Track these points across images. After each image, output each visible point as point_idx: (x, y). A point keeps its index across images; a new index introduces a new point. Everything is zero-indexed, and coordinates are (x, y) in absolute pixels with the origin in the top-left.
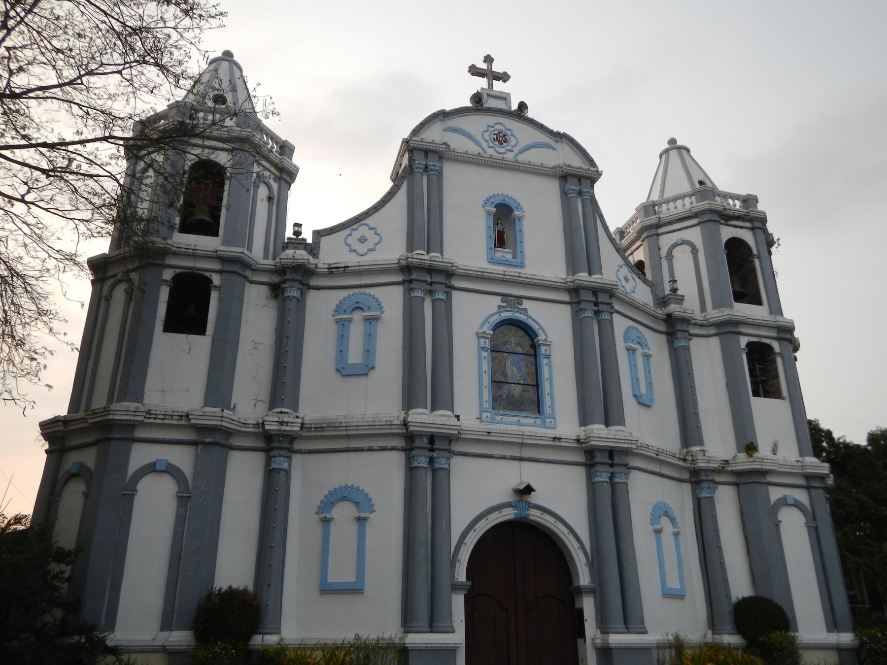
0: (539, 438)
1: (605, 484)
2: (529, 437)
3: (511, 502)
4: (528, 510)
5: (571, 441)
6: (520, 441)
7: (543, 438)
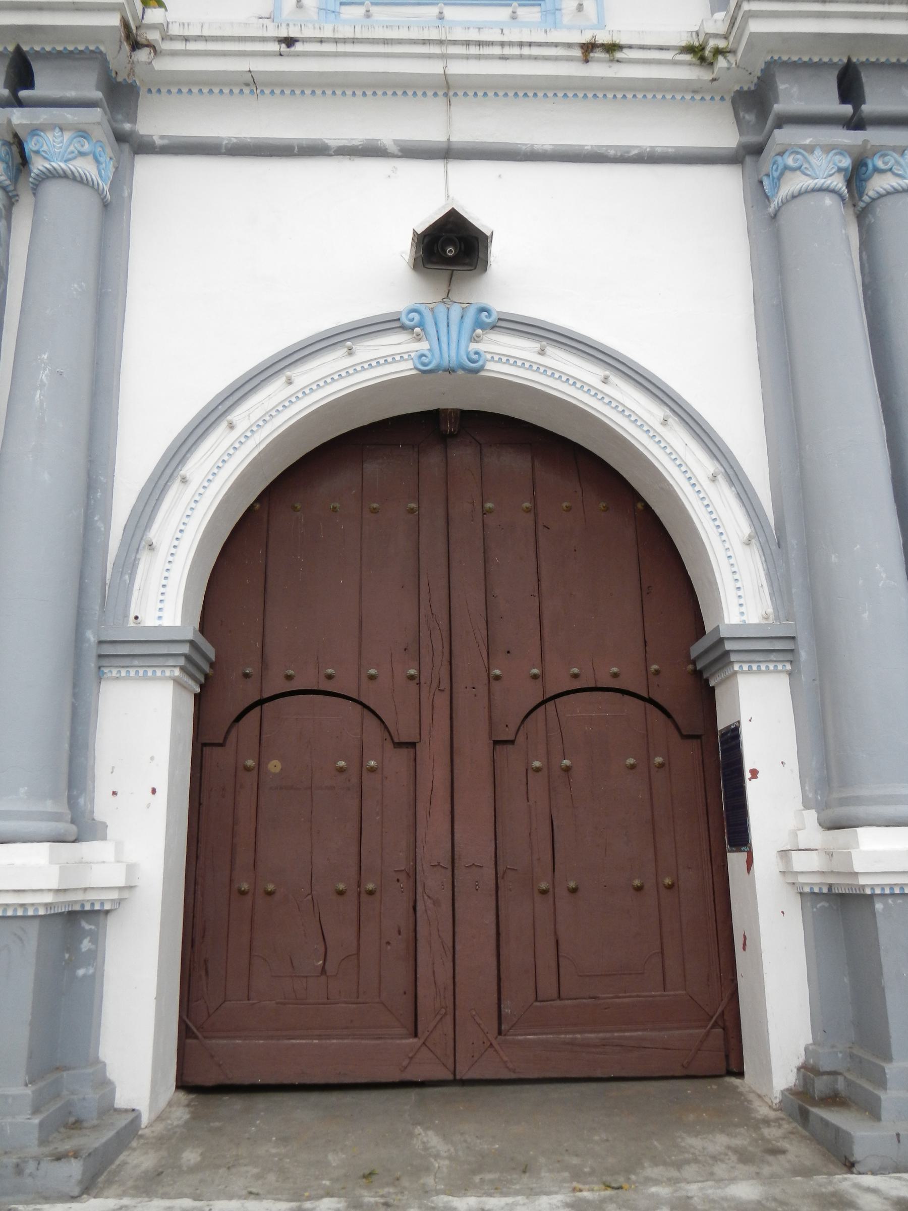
0: (516, 51)
1: (828, 201)
2: (474, 50)
3: (400, 313)
4: (475, 339)
5: (668, 55)
6: (435, 68)
7: (535, 51)
